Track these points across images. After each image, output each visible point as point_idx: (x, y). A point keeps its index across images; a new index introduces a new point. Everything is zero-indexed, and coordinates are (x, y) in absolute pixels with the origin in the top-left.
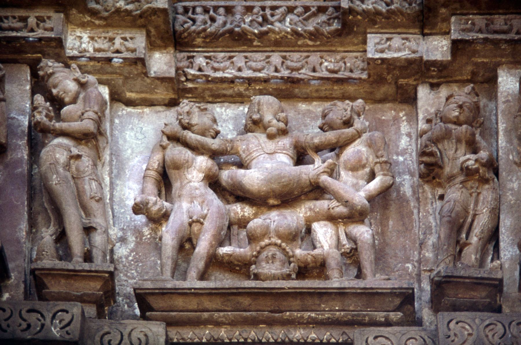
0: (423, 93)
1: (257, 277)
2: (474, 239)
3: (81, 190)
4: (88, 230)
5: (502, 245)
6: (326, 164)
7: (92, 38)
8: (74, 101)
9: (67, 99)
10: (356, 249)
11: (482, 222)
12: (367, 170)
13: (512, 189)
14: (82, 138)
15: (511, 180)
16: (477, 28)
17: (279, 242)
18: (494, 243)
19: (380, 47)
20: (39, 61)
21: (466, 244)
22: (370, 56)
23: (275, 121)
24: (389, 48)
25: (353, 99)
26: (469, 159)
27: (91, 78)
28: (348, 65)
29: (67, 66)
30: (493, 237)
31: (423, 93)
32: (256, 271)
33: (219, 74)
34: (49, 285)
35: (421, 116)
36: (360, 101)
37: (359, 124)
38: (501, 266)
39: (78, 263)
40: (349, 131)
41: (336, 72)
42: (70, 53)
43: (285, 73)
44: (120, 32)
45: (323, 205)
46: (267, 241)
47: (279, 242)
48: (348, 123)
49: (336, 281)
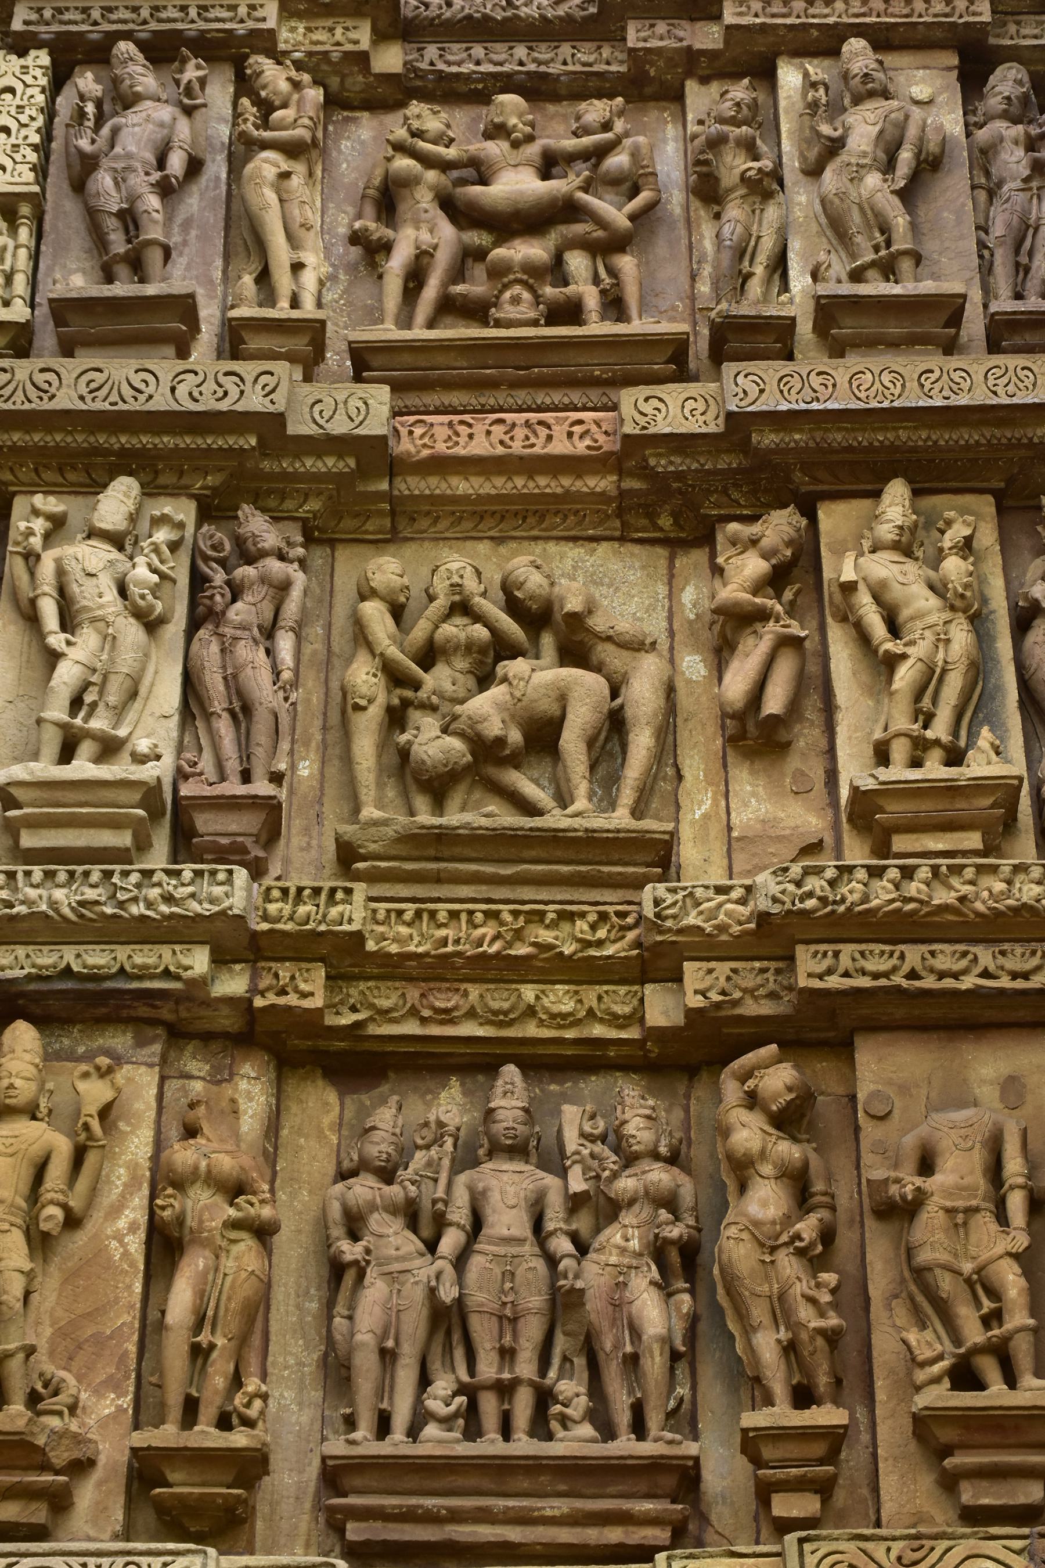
0: (691, 87)
1: (498, 324)
2: (759, 270)
3: (288, 215)
4: (297, 267)
5: (792, 273)
6: (581, 178)
7: (309, 29)
8: (285, 106)
9: (277, 103)
10: (618, 285)
11: (768, 245)
12: (628, 184)
13: (800, 204)
14: (292, 150)
15: (798, 193)
16: (753, 12)
17: (525, 277)
18: (779, 272)
19: (643, 34)
20: (246, 57)
21: (750, 275)
22: (630, 44)
23: (521, 125)
24: (653, 36)
25: (611, 97)
26: (750, 169)
27: (306, 78)
28: (604, 55)
29: (279, 63)
30: (780, 264)
31: (691, 87)
32: (497, 315)
33: (454, 69)
34: (246, 339)
35: (690, 117)
36: (620, 99)
37: (619, 126)
38: (791, 301)
39: (283, 310)
40: (609, 135)
41: (590, 65)
42: (282, 46)
43: (532, 67)
44: (342, 20)
45: (579, 229)
46: (512, 277)
47: (525, 277)
48: (607, 126)
49: (596, 327)
